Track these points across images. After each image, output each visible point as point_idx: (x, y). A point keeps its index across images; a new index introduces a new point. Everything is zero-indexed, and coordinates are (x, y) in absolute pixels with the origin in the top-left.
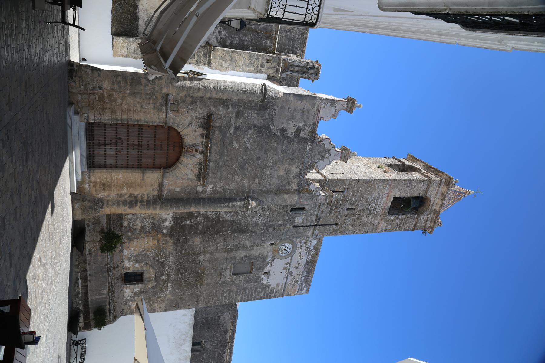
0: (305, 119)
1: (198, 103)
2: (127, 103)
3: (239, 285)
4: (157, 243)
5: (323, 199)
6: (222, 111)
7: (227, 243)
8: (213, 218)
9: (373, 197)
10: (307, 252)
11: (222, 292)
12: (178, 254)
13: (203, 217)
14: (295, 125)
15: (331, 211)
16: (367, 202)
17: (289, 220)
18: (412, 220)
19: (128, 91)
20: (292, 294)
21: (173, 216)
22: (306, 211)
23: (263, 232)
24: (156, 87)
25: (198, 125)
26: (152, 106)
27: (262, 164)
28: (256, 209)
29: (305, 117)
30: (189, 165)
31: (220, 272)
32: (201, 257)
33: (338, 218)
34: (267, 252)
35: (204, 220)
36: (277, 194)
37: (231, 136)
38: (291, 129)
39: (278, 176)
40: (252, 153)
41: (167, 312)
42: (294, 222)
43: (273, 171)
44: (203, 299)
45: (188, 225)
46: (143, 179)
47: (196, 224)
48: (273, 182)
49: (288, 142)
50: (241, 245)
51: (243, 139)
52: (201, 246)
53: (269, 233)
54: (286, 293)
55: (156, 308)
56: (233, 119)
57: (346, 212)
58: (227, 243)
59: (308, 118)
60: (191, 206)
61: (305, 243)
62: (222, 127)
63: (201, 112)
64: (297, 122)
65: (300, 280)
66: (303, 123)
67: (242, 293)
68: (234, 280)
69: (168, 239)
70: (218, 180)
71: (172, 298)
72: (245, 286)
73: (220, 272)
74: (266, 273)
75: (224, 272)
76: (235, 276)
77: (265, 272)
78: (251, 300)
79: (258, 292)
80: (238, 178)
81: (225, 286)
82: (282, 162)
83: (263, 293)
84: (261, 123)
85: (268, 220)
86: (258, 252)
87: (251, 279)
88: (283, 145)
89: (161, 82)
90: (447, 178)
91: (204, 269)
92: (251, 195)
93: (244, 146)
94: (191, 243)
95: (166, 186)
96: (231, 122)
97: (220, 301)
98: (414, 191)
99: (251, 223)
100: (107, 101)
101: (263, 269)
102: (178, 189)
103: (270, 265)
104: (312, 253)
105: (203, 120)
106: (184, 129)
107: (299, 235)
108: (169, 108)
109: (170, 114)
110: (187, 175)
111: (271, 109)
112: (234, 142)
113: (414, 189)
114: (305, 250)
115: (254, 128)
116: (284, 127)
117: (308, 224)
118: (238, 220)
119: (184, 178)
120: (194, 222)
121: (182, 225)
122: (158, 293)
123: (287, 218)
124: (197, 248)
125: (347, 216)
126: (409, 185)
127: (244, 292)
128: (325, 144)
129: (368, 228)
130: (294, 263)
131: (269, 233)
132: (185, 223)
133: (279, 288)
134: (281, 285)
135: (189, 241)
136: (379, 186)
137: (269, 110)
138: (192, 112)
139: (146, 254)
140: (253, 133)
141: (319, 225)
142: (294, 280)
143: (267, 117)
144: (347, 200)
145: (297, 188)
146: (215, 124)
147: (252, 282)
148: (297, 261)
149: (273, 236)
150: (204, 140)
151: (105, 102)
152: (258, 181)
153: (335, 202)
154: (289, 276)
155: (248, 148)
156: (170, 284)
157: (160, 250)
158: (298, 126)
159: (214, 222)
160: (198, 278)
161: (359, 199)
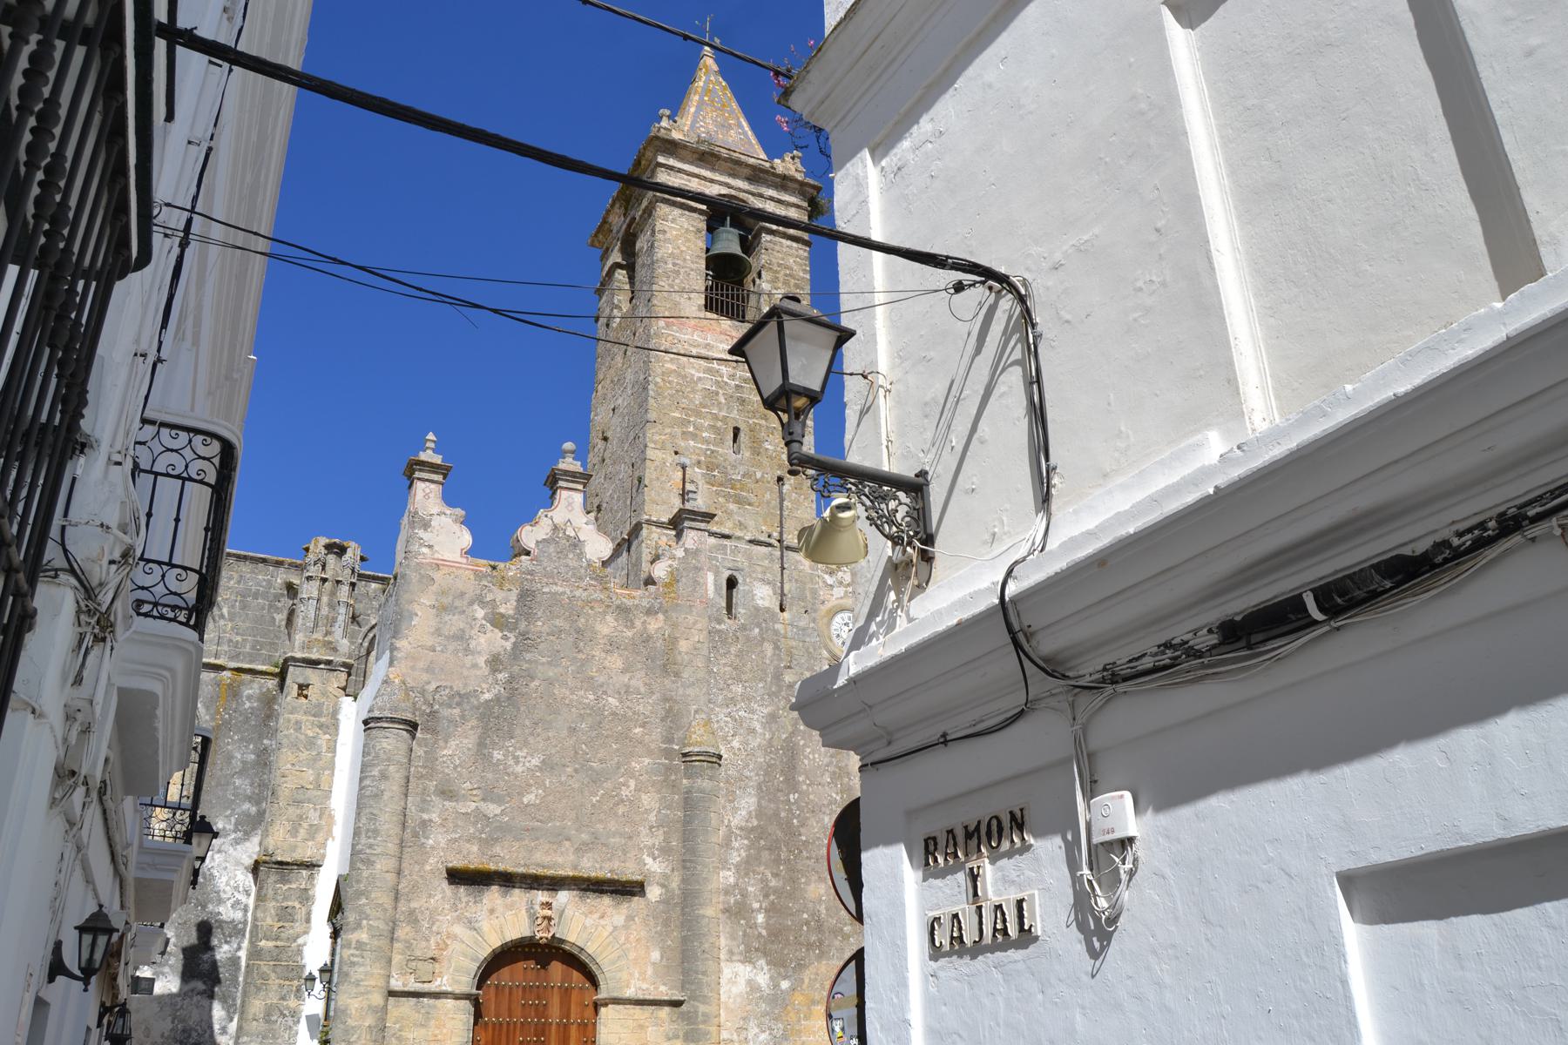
0: (465, 603)
1: (414, 905)
5: (696, 538)
6: (436, 839)
7: (825, 802)
8: (749, 848)
9: (702, 375)
13: (747, 874)
14: (482, 630)
15: (739, 501)
16: (717, 394)
18: (777, 248)
22: (735, 573)
24: (367, 1024)
25: (475, 902)
27: (590, 719)
28: (727, 722)
29: (457, 603)
33: (763, 476)
35: (754, 871)
38: (491, 641)
42: (768, 610)
43: (611, 687)
45: (768, 918)
47: (766, 896)
49: (528, 649)
50: (831, 763)
58: (825, 802)
59: (462, 594)
60: (704, 916)
62: (483, 836)
63: (439, 896)
66: (476, 607)
70: (630, 843)
80: (628, 787)
82: (584, 663)
85: (761, 685)
88: (536, 662)
89: (354, 1012)
92: (677, 747)
93: (538, 774)
95: (645, 986)
99: (767, 736)
102: (656, 955)
108: (426, 985)
109: (443, 983)
110: (615, 928)
112: (525, 800)
113: (684, 249)
115: (486, 748)
117: (777, 566)
118: (757, 775)
120: (759, 901)
121: (769, 935)
123: (757, 630)
125: (756, 451)
126: (670, 266)
128: (537, 542)
135: (815, 914)
137: (436, 707)
138: (438, 920)
141: (781, 533)
143: (457, 711)
145: (661, 616)
146: (472, 857)
152: (638, 730)
153: (715, 488)
155: (543, 762)
158: (484, 622)
159: (762, 842)
161: (710, 416)
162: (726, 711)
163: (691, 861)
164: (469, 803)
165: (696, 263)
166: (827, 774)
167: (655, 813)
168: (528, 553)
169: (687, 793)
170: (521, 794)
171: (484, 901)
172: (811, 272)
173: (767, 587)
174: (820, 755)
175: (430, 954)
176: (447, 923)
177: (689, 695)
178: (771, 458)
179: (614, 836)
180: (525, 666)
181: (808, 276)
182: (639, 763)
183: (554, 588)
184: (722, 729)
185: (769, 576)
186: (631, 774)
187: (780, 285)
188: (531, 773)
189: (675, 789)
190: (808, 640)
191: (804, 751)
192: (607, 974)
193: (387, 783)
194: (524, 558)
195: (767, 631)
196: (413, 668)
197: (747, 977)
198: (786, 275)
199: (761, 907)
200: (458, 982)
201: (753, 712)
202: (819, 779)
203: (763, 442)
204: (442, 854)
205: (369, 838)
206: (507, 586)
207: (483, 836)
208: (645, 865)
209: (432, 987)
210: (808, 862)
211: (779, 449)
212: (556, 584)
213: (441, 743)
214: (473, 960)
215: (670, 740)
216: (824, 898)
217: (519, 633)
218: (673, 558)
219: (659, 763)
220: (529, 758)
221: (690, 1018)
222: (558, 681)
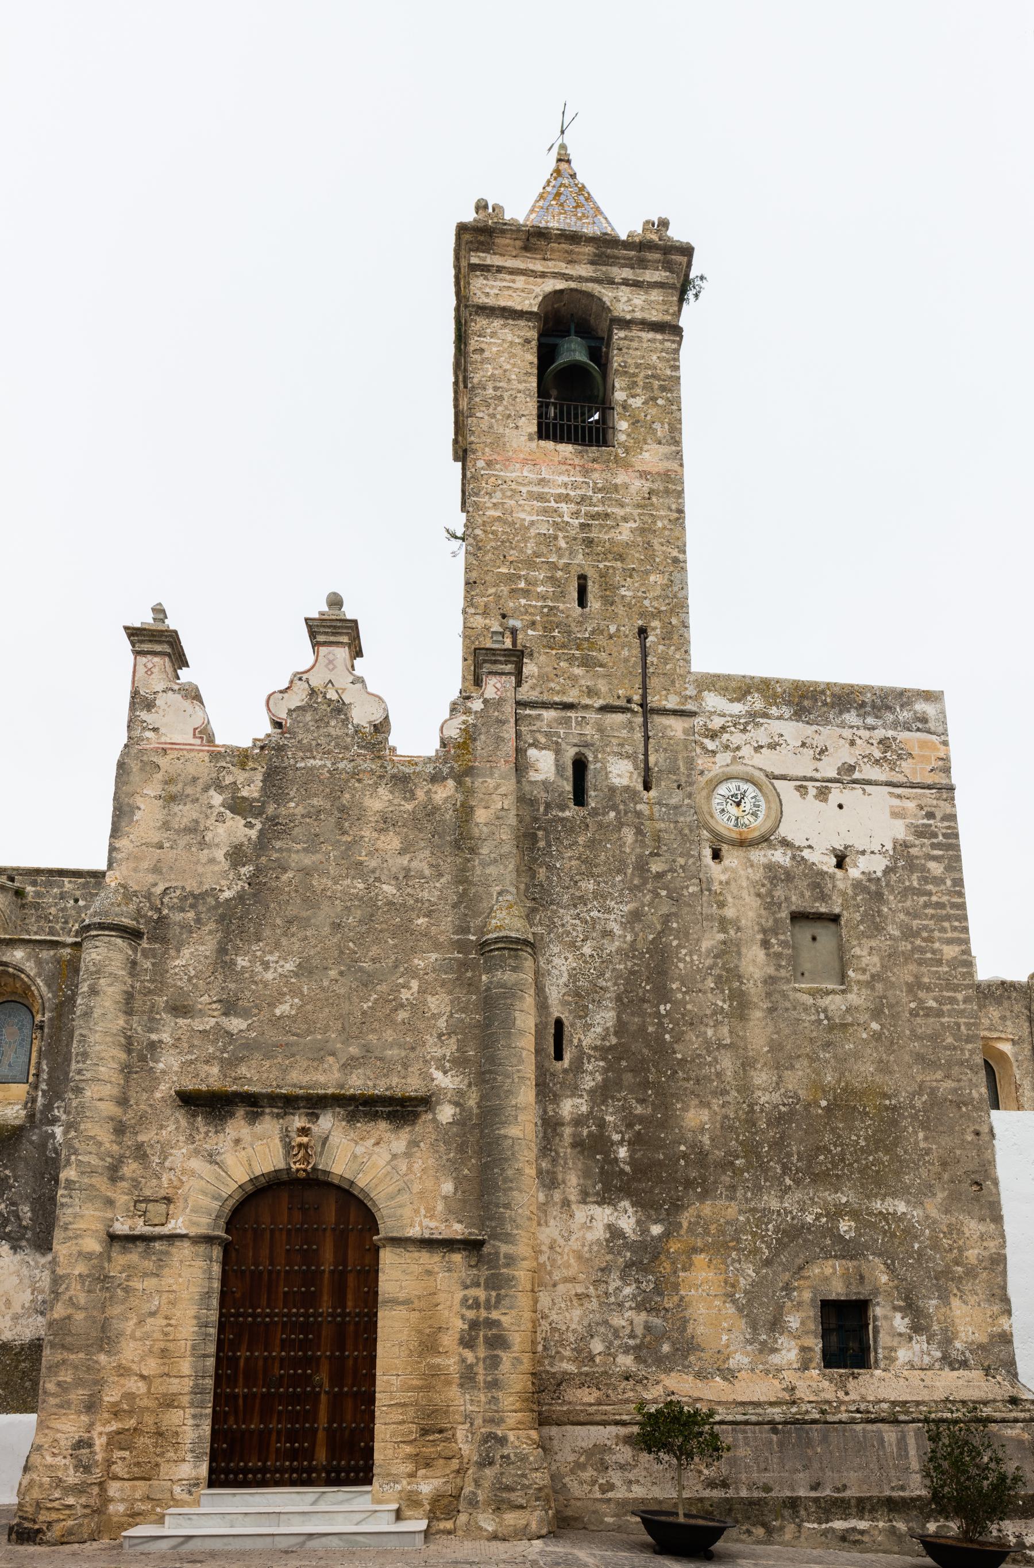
1: (141, 1138)
2: (142, 1359)
3: (890, 956)
6: (168, 1062)
7: (708, 1012)
11: (917, 1015)
20: (942, 755)
23: (664, 893)
25: (216, 1132)
26: (150, 1283)
27: (359, 912)
28: (575, 925)
30: (358, 1154)
31: (831, 1028)
32: (762, 1101)
34: (750, 870)
36: (473, 850)
39: (401, 852)
40: (318, 949)
41: (1004, 1212)
42: (627, 789)
43: (386, 872)
44: (949, 1084)
46: (407, 1302)
48: (427, 867)
50: (715, 964)
51: (266, 985)
53: (669, 871)
54: (939, 778)
55: (986, 1254)
56: (198, 1025)
57: (594, 604)
58: (708, 1012)
61: (713, 735)
62: (225, 1055)
63: (172, 1127)
64: (209, 811)
65: (880, 733)
67: (924, 940)
68: (866, 977)
70: (412, 1055)
71: (940, 1196)
72: (897, 933)
73: (831, 1028)
74: (841, 863)
75: (830, 1014)
76: (851, 973)
78: (962, 906)
79: (927, 883)
80: (410, 988)
81: (891, 1006)
83: (932, 865)
84: (210, 932)
85: (619, 878)
86: (748, 899)
87: (865, 914)
88: (289, 850)
91: (818, 1087)
92: (473, 938)
95: (433, 1224)
96: (208, 1027)
97: (964, 1020)
100: (132, 1423)
101: (822, 874)
102: (448, 1187)
103: (806, 854)
105: (200, 1119)
106: (230, 1176)
107: (681, 763)
109: (177, 1225)
110: (395, 1156)
111: (162, 903)
112: (277, 1012)
114: (744, 730)
116: (227, 855)
118: (615, 984)
119: (404, 1168)
122: (916, 1246)
123: (612, 814)
127: (925, 934)
129: (662, 513)
130: (803, 766)
131: (669, 871)
133: (911, 805)
134: (896, 802)
137: (165, 912)
138: (171, 1155)
140: (245, 955)
142: (877, 754)
143: (191, 915)
146: (211, 1080)
147: (879, 912)
148: (790, 754)
149: (681, 855)
150: (267, 1110)
151: (135, 1429)
152: (420, 921)
154: (857, 775)
156: (877, 1205)
160: (855, 1108)
163: (490, 1072)
164: (207, 1019)
166: (710, 979)
167: (445, 1018)
169: (486, 991)
170: (272, 1005)
171: (227, 1130)
173: (626, 762)
174: (700, 956)
175: (162, 1193)
176: (179, 1155)
177: (490, 875)
178: (630, 606)
179: (391, 1046)
180: (275, 856)
182: (423, 959)
184: (568, 933)
186: (413, 973)
188: (284, 980)
189: (472, 988)
190: (682, 819)
191: (677, 953)
192: (384, 1212)
195: (626, 813)
196: (135, 870)
200: (197, 1224)
201: (609, 911)
202: (699, 986)
203: (618, 588)
207: (225, 1055)
208: (433, 1080)
209: (165, 1230)
210: (686, 1085)
211: (640, 594)
213: (173, 953)
214: (215, 1198)
215: (464, 930)
216: (707, 1127)
217: (267, 818)
219: (451, 959)
220: (281, 963)
221: (492, 1261)
222: (316, 870)
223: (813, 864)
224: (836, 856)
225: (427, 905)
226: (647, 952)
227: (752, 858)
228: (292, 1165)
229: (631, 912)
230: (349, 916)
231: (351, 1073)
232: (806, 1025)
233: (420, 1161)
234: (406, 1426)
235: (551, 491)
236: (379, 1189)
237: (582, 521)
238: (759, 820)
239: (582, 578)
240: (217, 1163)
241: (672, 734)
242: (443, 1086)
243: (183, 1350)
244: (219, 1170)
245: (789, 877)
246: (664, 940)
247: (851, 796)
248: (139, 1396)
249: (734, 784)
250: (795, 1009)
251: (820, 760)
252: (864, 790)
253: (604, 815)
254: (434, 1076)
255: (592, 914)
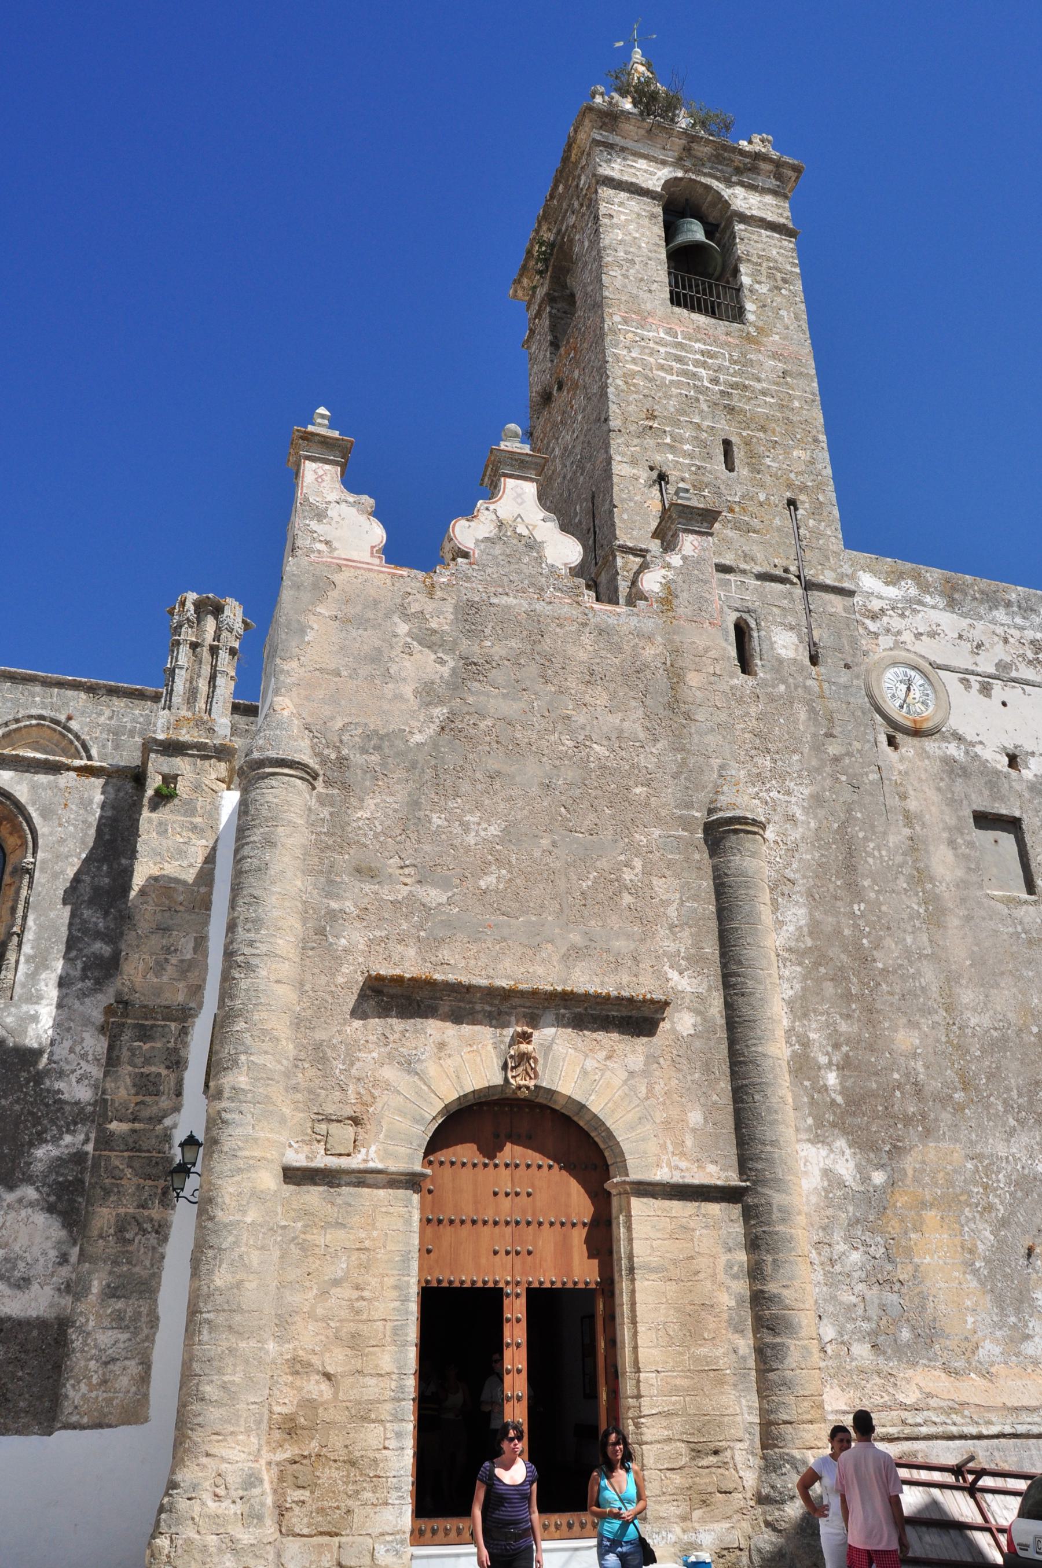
1: (320, 1035)
4: (933, 1213)
5: (696, 543)
8: (805, 978)
9: (674, 378)
10: (914, 610)
12: (970, 1118)
13: (805, 1015)
14: (407, 650)
16: (697, 400)
17: (791, 680)
19: (271, 1346)
21: (809, 1140)
22: (745, 616)
23: (844, 778)
26: (335, 1237)
29: (370, 614)
30: (589, 1069)
33: (767, 499)
34: (927, 762)
35: (815, 1011)
37: (456, 897)
40: (526, 812)
45: (843, 1079)
47: (836, 1046)
48: (640, 729)
50: (905, 863)
51: (468, 850)
52: (925, 1024)
57: (742, 470)
59: (376, 603)
61: (874, 617)
66: (396, 619)
69: (909, 1163)
77: (1010, 766)
84: (399, 781)
85: (796, 757)
90: (587, 122)
93: (498, 847)
94: (919, 1066)
96: (400, 897)
98: (643, 235)
99: (812, 825)
101: (997, 773)
102: (695, 1117)
103: (978, 749)
104: (913, 592)
111: (341, 741)
112: (483, 884)
113: (637, 235)
114: (902, 616)
116: (416, 692)
117: (800, 607)
119: (644, 1090)
120: (827, 1054)
121: (848, 1104)
123: (782, 688)
124: (938, 1041)
125: (755, 470)
126: (622, 254)
128: (477, 541)
132: (835, 1091)
136: (634, 359)
137: (345, 752)
139: (988, 1261)
140: (441, 812)
142: (1030, 655)
143: (375, 758)
144: (693, 469)
148: (949, 645)
154: (1014, 674)
157: (963, 1198)
158: (409, 640)
159: (822, 970)
162: (752, 790)
165: (655, 252)
166: (902, 878)
167: (675, 905)
168: (465, 555)
172: (801, 265)
173: (790, 634)
174: (888, 851)
181: (797, 270)
183: (504, 600)
185: (790, 620)
187: (764, 279)
188: (488, 845)
190: (852, 700)
191: (865, 847)
193: (274, 850)
194: (460, 560)
195: (796, 687)
197: (822, 1165)
198: (770, 268)
199: (830, 1063)
200: (396, 1157)
201: (789, 793)
204: (361, 960)
205: (248, 931)
206: (439, 594)
209: (355, 1162)
211: (785, 466)
212: (507, 594)
214: (416, 1120)
218: (668, 566)
220: (484, 825)
223: (987, 761)
224: (1008, 755)
225: (644, 771)
226: (834, 843)
227: (928, 749)
228: (512, 1081)
229: (812, 796)
230: (558, 776)
231: (575, 966)
232: (1006, 937)
233: (662, 1082)
234: (674, 1445)
235: (691, 356)
236: (617, 1115)
237: (722, 388)
238: (931, 709)
239: (727, 444)
240: (417, 1074)
241: (833, 610)
242: (679, 988)
243: (381, 1336)
244: (419, 1083)
245: (965, 773)
246: (849, 830)
247: (1013, 694)
248: (322, 1404)
249: (902, 669)
250: (991, 919)
251: (978, 654)
252: (1023, 689)
253: (774, 687)
254: (670, 976)
255: (771, 794)
